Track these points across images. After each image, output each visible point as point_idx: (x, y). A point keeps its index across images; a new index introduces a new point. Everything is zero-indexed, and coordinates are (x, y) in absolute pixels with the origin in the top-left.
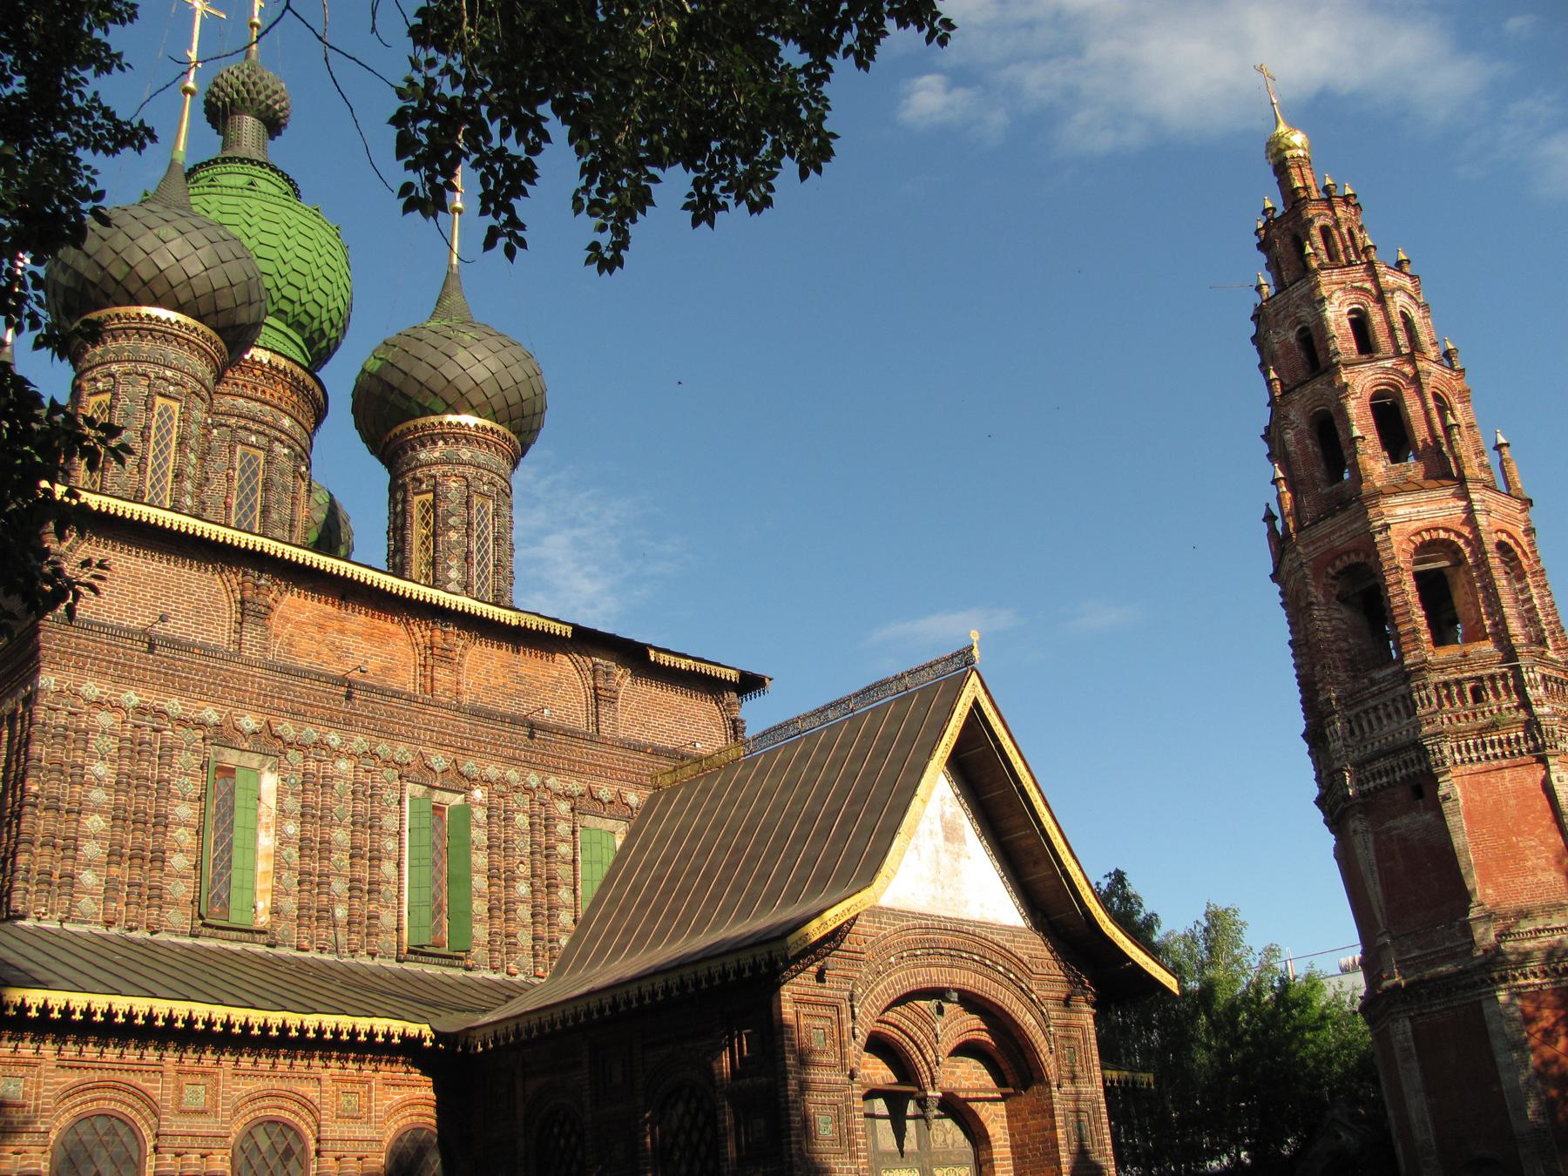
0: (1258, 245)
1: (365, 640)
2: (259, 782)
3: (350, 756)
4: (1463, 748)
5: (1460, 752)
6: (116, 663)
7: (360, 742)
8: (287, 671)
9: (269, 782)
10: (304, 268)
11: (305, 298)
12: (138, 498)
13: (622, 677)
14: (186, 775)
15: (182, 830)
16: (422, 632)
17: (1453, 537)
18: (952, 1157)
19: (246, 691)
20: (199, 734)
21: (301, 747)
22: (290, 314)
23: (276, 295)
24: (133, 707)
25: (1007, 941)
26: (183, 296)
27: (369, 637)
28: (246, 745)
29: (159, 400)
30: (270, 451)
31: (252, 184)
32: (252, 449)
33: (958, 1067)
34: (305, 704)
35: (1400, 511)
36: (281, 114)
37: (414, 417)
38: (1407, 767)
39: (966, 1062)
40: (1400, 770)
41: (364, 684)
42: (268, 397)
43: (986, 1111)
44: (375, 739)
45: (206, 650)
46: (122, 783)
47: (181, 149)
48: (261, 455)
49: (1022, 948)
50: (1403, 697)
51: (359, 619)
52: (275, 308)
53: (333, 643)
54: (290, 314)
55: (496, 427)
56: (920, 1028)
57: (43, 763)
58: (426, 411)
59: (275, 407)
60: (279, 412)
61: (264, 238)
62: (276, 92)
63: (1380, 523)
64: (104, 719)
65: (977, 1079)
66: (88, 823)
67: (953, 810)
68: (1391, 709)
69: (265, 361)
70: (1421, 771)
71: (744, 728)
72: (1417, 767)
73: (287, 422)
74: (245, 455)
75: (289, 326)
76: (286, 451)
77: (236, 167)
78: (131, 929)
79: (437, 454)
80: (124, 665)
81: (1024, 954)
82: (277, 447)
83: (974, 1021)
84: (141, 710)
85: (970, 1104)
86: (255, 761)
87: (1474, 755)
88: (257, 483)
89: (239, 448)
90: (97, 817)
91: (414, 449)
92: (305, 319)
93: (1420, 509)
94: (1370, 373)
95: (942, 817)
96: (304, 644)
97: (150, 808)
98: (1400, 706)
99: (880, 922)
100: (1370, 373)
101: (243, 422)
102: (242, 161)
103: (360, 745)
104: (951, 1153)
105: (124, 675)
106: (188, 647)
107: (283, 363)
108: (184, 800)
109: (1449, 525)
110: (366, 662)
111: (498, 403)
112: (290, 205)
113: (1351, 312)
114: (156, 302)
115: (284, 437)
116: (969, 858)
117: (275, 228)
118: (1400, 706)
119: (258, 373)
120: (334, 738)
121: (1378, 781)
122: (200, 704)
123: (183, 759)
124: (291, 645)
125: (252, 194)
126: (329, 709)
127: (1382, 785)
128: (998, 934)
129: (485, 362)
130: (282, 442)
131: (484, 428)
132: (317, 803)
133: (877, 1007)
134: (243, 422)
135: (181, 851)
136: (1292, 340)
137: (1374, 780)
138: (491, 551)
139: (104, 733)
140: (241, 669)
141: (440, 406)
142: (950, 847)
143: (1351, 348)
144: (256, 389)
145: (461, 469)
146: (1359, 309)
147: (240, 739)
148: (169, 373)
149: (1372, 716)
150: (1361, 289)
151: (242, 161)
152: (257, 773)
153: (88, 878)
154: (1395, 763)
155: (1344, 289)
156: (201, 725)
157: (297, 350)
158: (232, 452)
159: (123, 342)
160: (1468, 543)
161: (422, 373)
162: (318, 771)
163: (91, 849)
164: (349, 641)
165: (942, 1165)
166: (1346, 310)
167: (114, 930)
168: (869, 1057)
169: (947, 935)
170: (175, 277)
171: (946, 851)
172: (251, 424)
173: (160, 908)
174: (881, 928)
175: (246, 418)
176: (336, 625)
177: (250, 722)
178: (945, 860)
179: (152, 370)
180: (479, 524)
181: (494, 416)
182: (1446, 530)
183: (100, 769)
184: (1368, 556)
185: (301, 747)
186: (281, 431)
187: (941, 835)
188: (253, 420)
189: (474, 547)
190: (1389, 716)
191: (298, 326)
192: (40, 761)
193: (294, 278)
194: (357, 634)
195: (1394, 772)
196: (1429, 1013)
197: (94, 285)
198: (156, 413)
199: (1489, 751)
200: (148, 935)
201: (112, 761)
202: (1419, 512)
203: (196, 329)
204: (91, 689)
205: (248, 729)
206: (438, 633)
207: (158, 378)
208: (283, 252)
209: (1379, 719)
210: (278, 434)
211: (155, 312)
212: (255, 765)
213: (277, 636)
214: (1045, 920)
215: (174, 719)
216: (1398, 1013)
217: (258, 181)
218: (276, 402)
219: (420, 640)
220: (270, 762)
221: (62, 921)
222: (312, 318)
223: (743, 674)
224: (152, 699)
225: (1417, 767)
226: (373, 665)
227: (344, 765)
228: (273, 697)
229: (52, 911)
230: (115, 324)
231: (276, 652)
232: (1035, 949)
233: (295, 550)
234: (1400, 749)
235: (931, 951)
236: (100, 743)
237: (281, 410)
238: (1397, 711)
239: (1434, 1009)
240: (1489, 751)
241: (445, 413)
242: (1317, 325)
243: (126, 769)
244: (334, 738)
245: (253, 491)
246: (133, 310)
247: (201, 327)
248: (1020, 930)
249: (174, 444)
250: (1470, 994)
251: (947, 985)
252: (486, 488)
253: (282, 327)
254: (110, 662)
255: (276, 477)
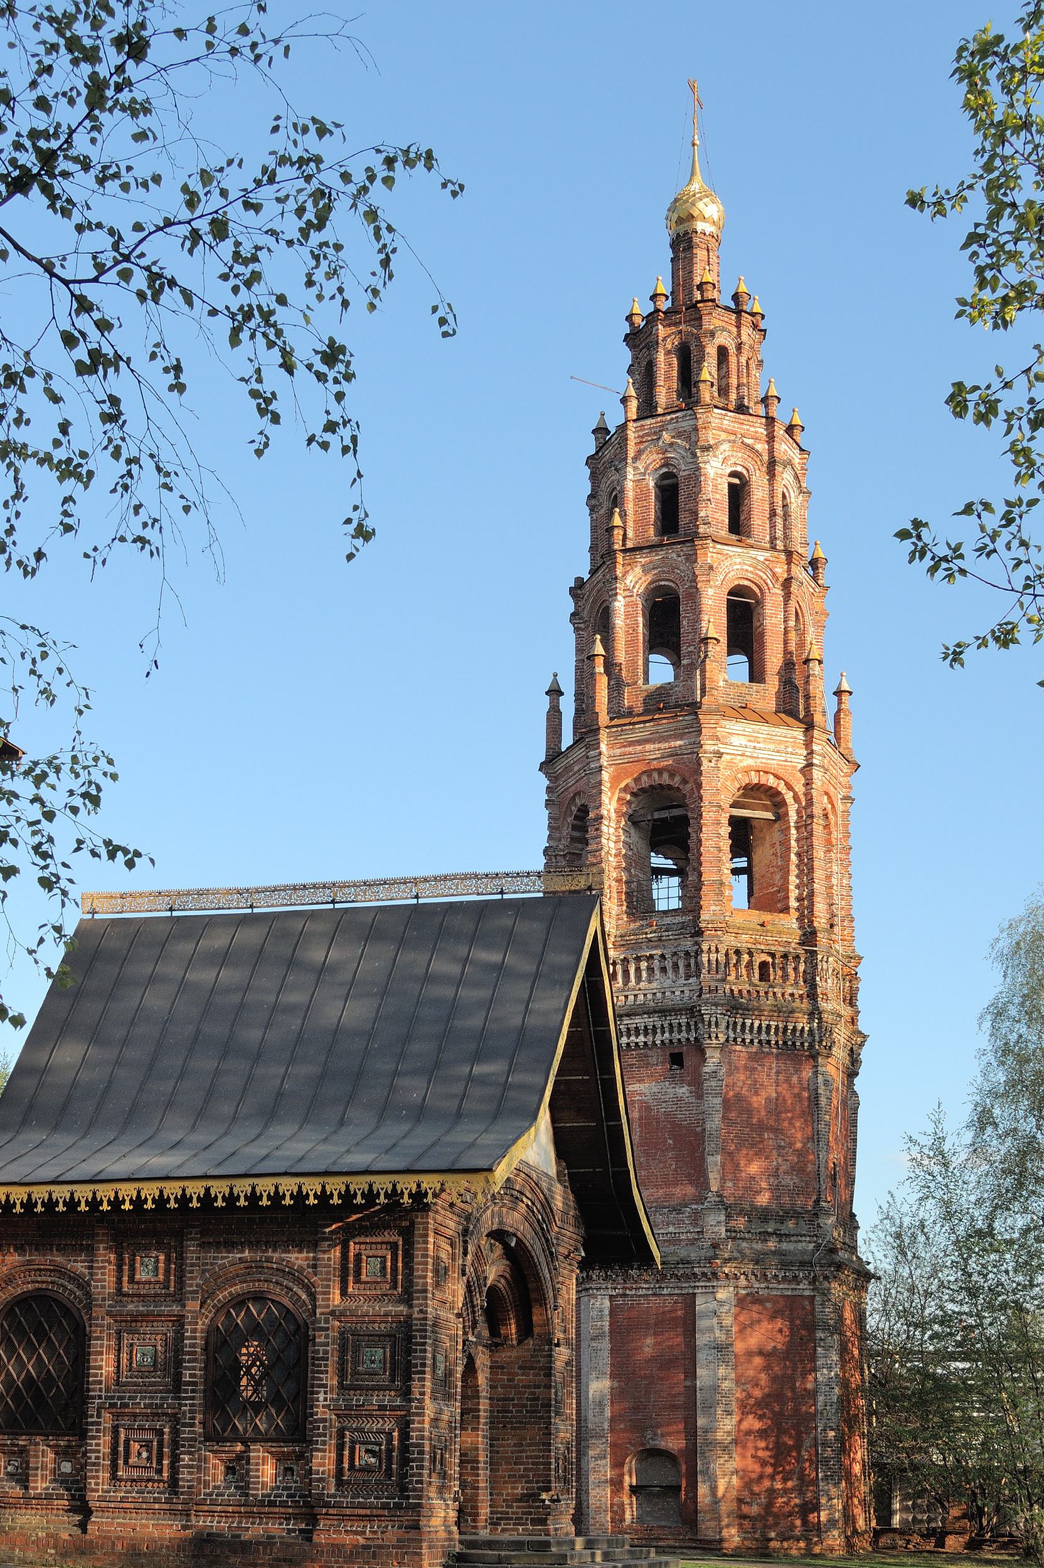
0: (627, 336)
4: (739, 1027)
5: (734, 1030)
17: (782, 788)
35: (735, 740)
38: (671, 1032)
40: (663, 1033)
50: (687, 954)
63: (712, 748)
68: (669, 964)
70: (688, 1039)
72: (684, 1034)
87: (748, 1037)
93: (758, 745)
94: (738, 561)
98: (681, 964)
100: (738, 561)
109: (781, 773)
113: (734, 474)
118: (681, 964)
121: (633, 1038)
127: (637, 1043)
136: (652, 484)
137: (629, 1036)
143: (722, 522)
146: (741, 473)
149: (644, 965)
150: (751, 448)
154: (658, 1024)
155: (734, 442)
160: (796, 798)
166: (729, 470)
182: (776, 776)
184: (685, 781)
190: (664, 970)
195: (655, 1033)
196: (632, 1296)
199: (764, 1036)
202: (755, 748)
209: (650, 969)
216: (598, 1289)
225: (684, 1034)
234: (670, 1011)
238: (676, 966)
239: (641, 1292)
240: (764, 1036)
242: (689, 477)
250: (686, 1285)
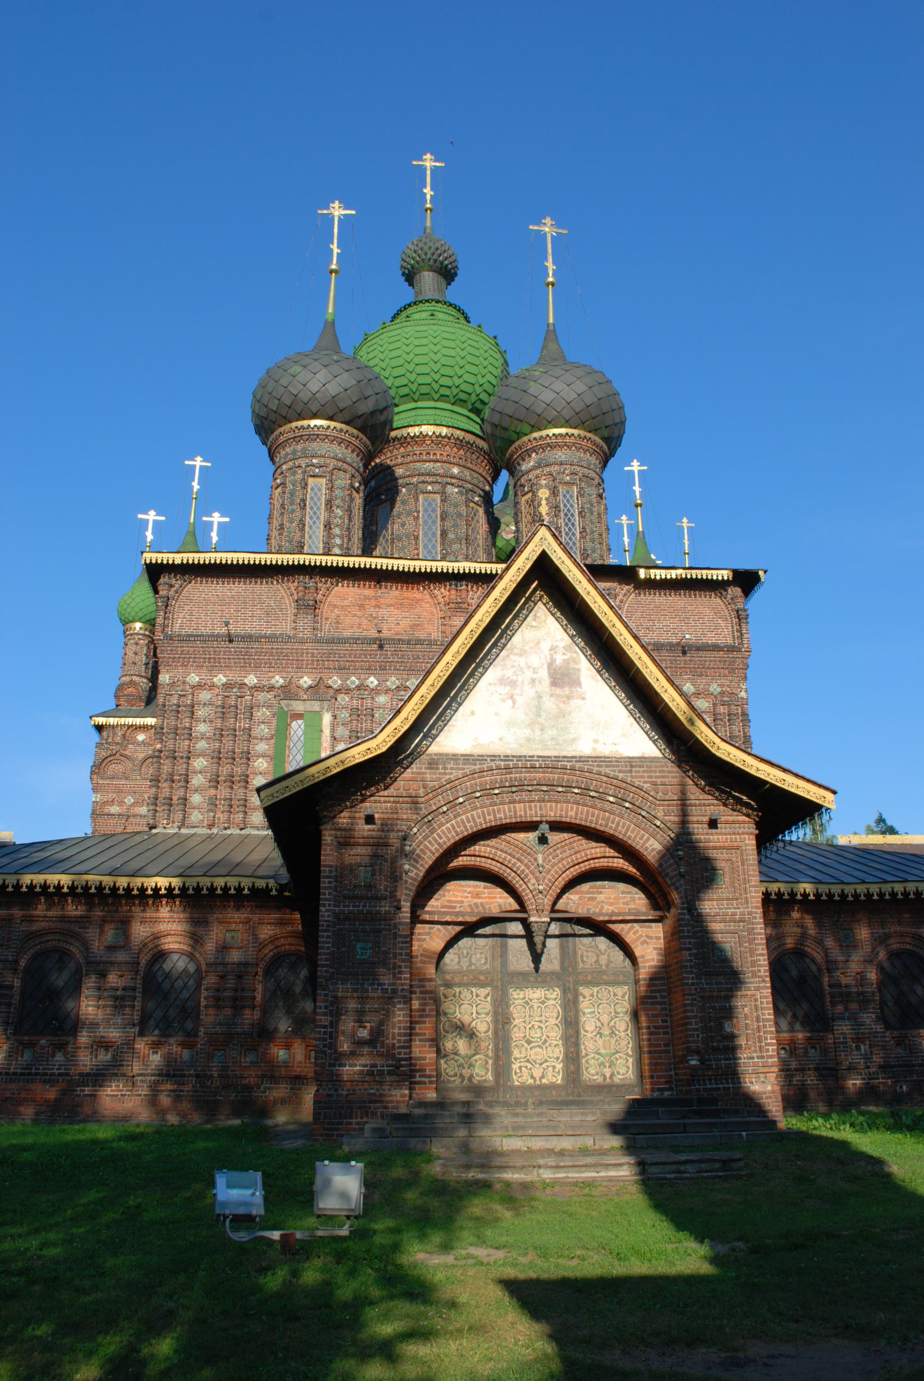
1: (398, 608)
2: (321, 720)
3: (387, 691)
6: (209, 658)
7: (393, 682)
8: (331, 641)
9: (327, 718)
10: (451, 362)
11: (457, 382)
12: (300, 550)
13: (625, 595)
14: (263, 723)
15: (260, 760)
16: (442, 592)
18: (605, 977)
19: (303, 660)
20: (269, 696)
21: (348, 691)
22: (451, 396)
23: (436, 387)
24: (223, 685)
25: (620, 771)
26: (314, 408)
27: (400, 606)
28: (305, 697)
29: (311, 481)
30: (443, 493)
31: (432, 315)
32: (431, 495)
33: (601, 893)
34: (349, 661)
36: (446, 262)
37: (514, 442)
39: (612, 888)
41: (394, 640)
42: (438, 457)
43: (635, 933)
44: (405, 676)
45: (271, 638)
46: (220, 734)
47: (330, 310)
48: (438, 497)
49: (643, 777)
51: (392, 593)
52: (438, 395)
53: (371, 615)
54: (451, 396)
55: (570, 431)
56: (518, 859)
57: (165, 731)
58: (519, 435)
59: (444, 462)
60: (448, 465)
61: (418, 351)
62: (438, 249)
64: (205, 696)
65: (626, 903)
66: (196, 764)
67: (566, 657)
69: (430, 434)
71: (748, 615)
73: (455, 470)
74: (426, 500)
75: (453, 404)
76: (456, 490)
77: (421, 307)
78: (225, 829)
79: (532, 463)
80: (215, 659)
81: (645, 782)
82: (449, 489)
83: (599, 849)
84: (227, 686)
85: (610, 926)
86: (316, 706)
88: (436, 517)
89: (421, 497)
90: (201, 759)
91: (519, 465)
92: (463, 396)
95: (550, 665)
96: (348, 620)
97: (239, 748)
99: (445, 768)
101: (422, 478)
102: (427, 301)
103: (394, 683)
104: (604, 973)
105: (215, 665)
106: (257, 638)
107: (444, 431)
108: (262, 739)
110: (398, 624)
111: (567, 414)
112: (435, 322)
114: (315, 416)
115: (454, 481)
116: (583, 699)
117: (424, 341)
119: (428, 442)
120: (373, 681)
122: (271, 674)
123: (261, 713)
124: (338, 623)
125: (408, 323)
126: (368, 661)
128: (607, 766)
129: (551, 387)
130: (452, 485)
131: (561, 435)
132: (361, 728)
133: (439, 844)
134: (422, 478)
135: (261, 773)
138: (577, 523)
139: (205, 704)
140: (296, 646)
141: (526, 428)
142: (558, 691)
144: (429, 453)
145: (548, 469)
147: (302, 693)
148: (315, 461)
151: (427, 301)
152: (319, 715)
153: (196, 799)
156: (271, 688)
157: (465, 420)
158: (417, 500)
159: (288, 450)
161: (509, 409)
162: (362, 706)
163: (197, 780)
164: (383, 612)
165: (589, 984)
167: (215, 831)
168: (485, 888)
169: (536, 772)
170: (305, 396)
171: (551, 695)
172: (428, 479)
173: (246, 813)
174: (445, 774)
175: (423, 475)
176: (373, 603)
177: (306, 681)
178: (549, 704)
179: (303, 462)
180: (565, 506)
181: (567, 423)
183: (202, 728)
185: (348, 691)
186: (451, 477)
187: (546, 680)
188: (428, 475)
189: (561, 522)
191: (459, 402)
192: (163, 729)
193: (444, 371)
194: (390, 605)
197: (266, 418)
198: (309, 490)
200: (238, 831)
201: (211, 721)
203: (329, 427)
204: (194, 678)
205: (305, 686)
206: (453, 592)
207: (308, 466)
208: (405, 356)
210: (449, 480)
211: (314, 423)
212: (317, 708)
213: (327, 619)
214: (682, 748)
215: (252, 688)
217: (436, 313)
218: (445, 459)
219: (441, 600)
220: (326, 704)
221: (180, 828)
222: (470, 394)
223: (736, 573)
224: (235, 676)
226: (405, 623)
227: (382, 699)
228: (323, 661)
229: (173, 822)
230: (282, 439)
231: (327, 629)
232: (671, 774)
233: (286, 557)
235: (514, 789)
236: (201, 712)
237: (450, 463)
241: (531, 432)
243: (219, 725)
244: (373, 681)
245: (434, 522)
246: (288, 426)
247: (333, 424)
248: (653, 759)
249: (323, 505)
251: (538, 819)
252: (568, 478)
253: (448, 406)
254: (205, 658)
255: (451, 510)
